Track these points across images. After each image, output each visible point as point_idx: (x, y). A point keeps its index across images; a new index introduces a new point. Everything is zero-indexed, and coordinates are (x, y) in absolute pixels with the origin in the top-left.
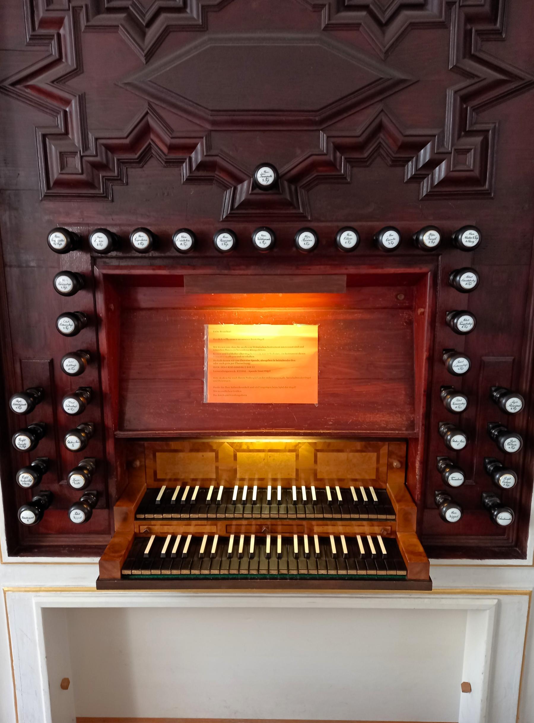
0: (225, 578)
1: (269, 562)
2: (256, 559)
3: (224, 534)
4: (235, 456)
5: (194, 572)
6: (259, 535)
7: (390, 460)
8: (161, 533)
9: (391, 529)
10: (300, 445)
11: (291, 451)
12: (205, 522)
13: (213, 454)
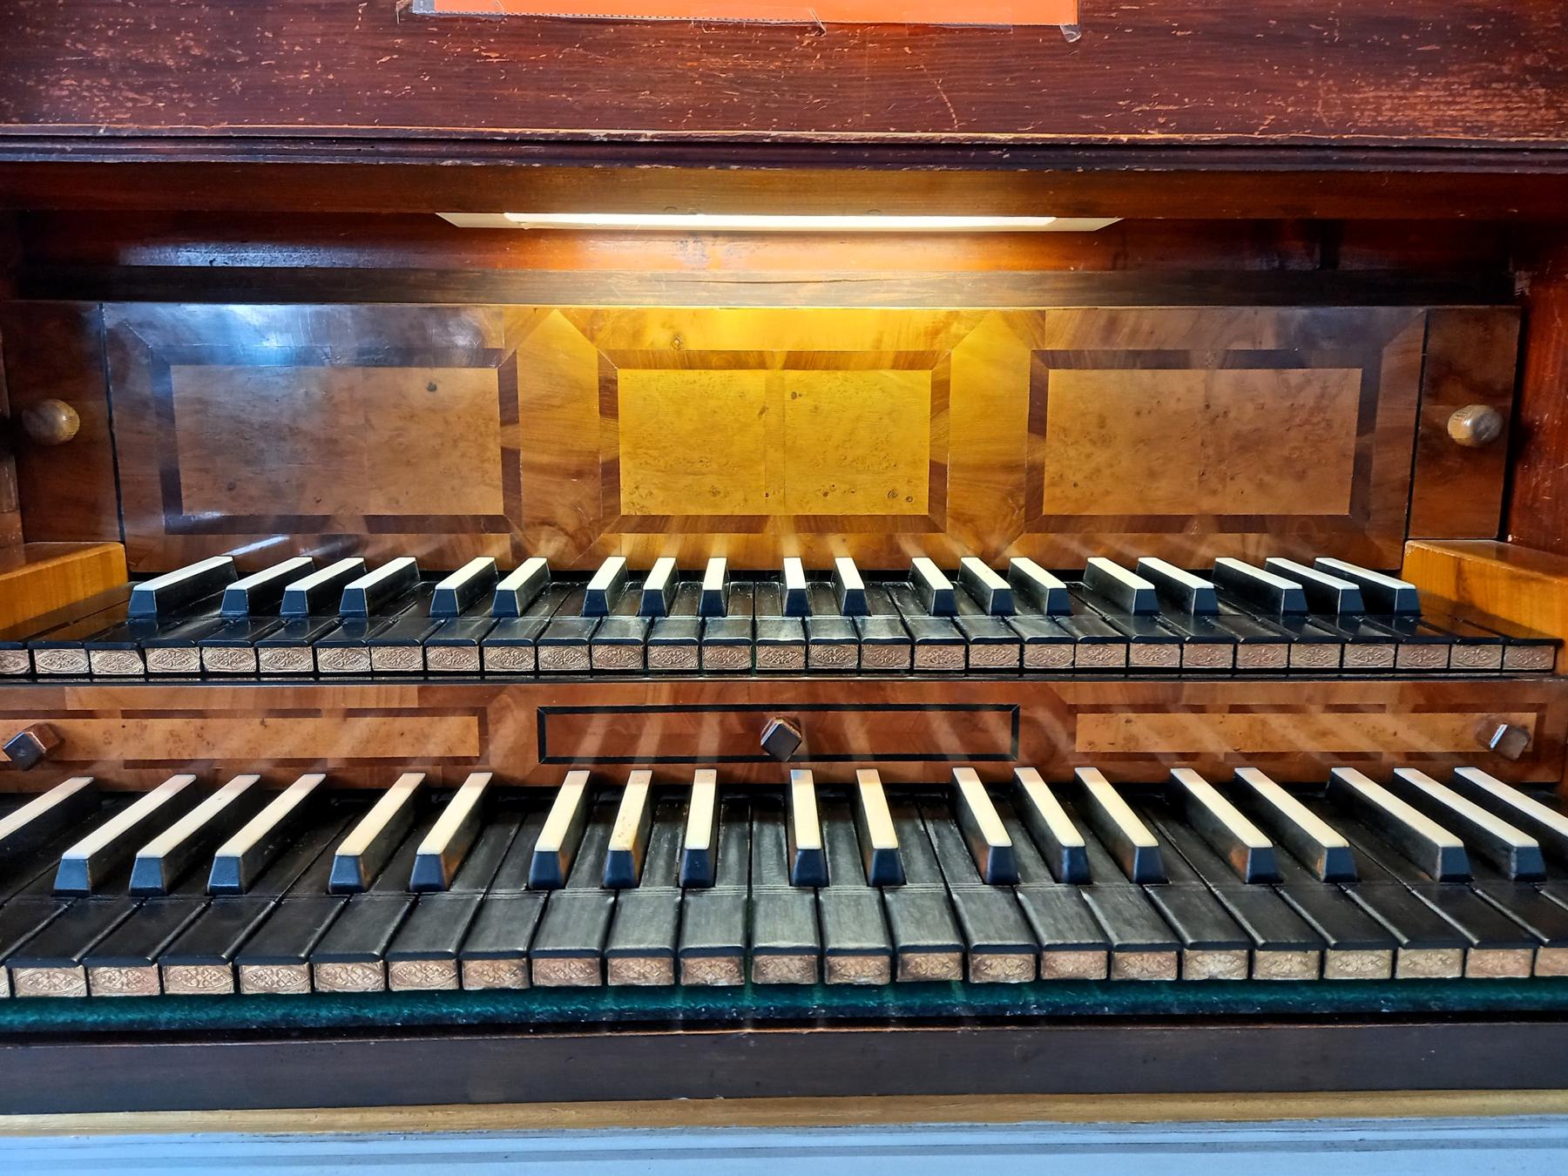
0: (497, 1019)
1: (817, 907)
2: (726, 889)
3: (526, 768)
4: (608, 388)
5: (262, 978)
6: (740, 770)
7: (1432, 409)
8: (130, 764)
9: (1540, 722)
10: (955, 328)
11: (910, 361)
12: (410, 695)
13: (489, 377)
